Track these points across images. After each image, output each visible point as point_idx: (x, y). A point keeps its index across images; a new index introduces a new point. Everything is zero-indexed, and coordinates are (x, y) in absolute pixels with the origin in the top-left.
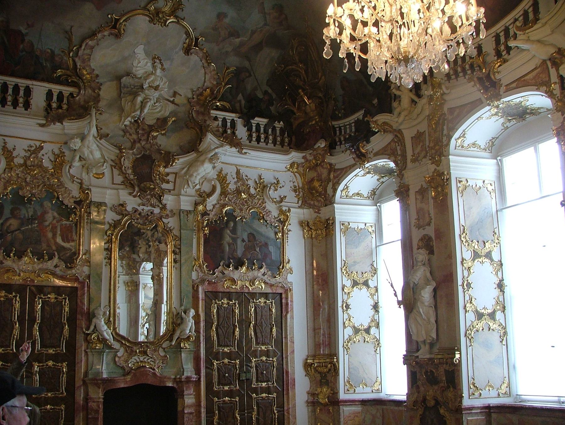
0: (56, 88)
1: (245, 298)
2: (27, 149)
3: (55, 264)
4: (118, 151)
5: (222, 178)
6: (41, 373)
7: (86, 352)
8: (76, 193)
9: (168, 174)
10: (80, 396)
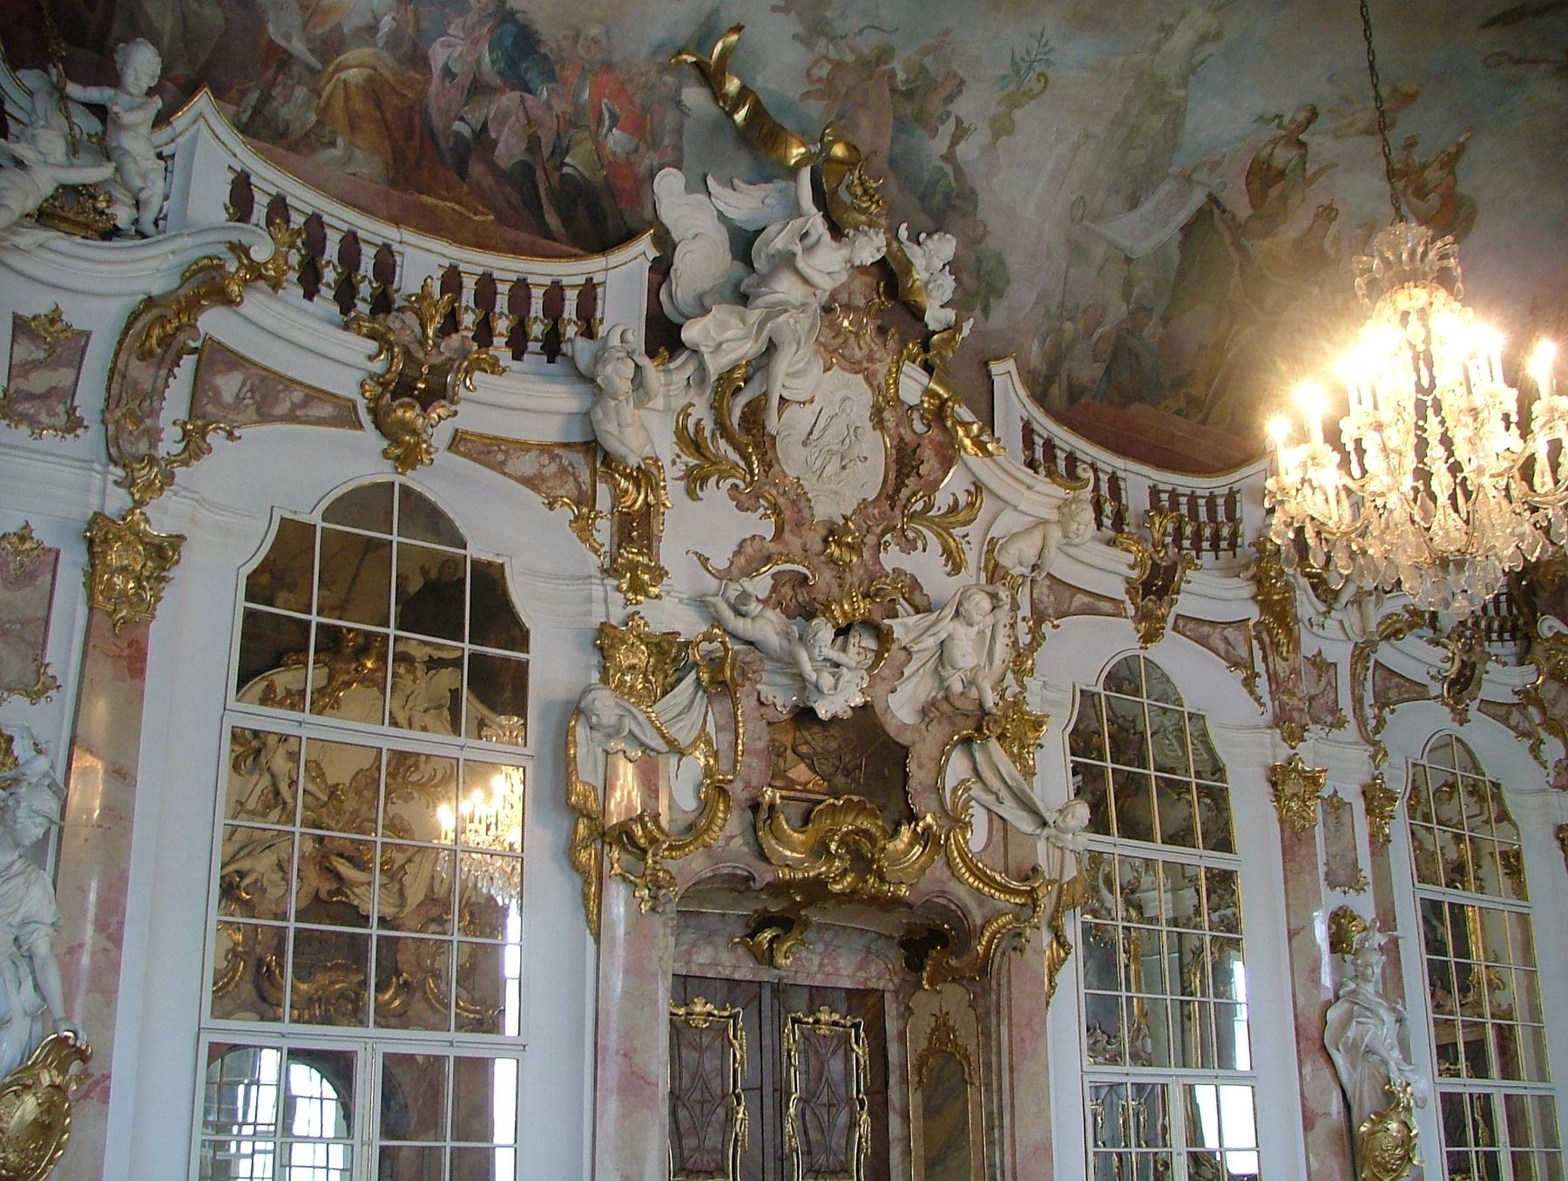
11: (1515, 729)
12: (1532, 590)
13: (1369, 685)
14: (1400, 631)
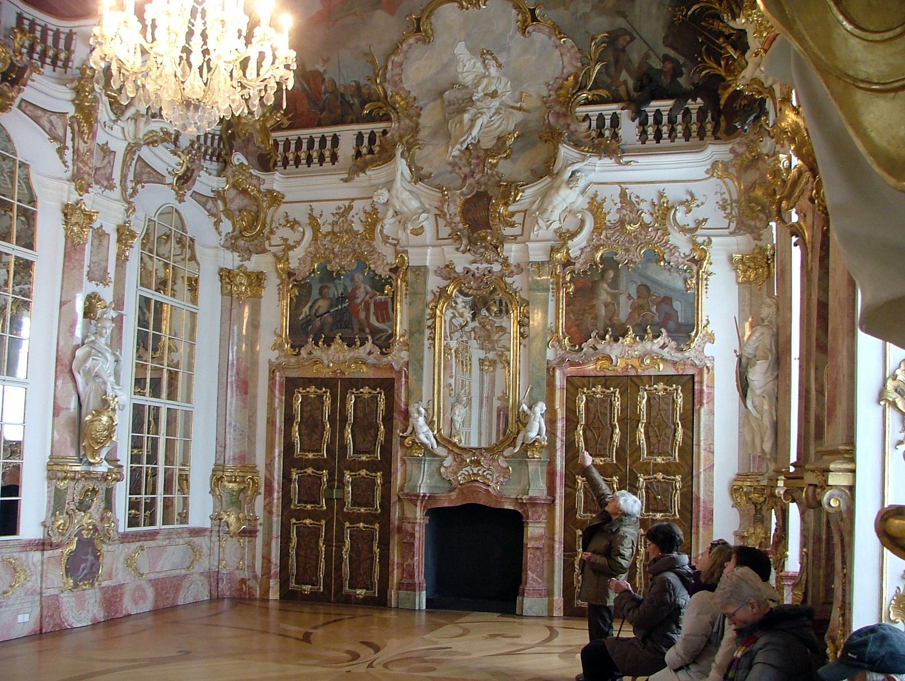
0: (366, 128)
1: (629, 383)
2: (335, 212)
4: (441, 195)
5: (596, 207)
6: (354, 484)
8: (391, 259)
9: (512, 214)
10: (396, 513)
11: (208, 211)
12: (232, 137)
13: (132, 169)
14: (156, 141)
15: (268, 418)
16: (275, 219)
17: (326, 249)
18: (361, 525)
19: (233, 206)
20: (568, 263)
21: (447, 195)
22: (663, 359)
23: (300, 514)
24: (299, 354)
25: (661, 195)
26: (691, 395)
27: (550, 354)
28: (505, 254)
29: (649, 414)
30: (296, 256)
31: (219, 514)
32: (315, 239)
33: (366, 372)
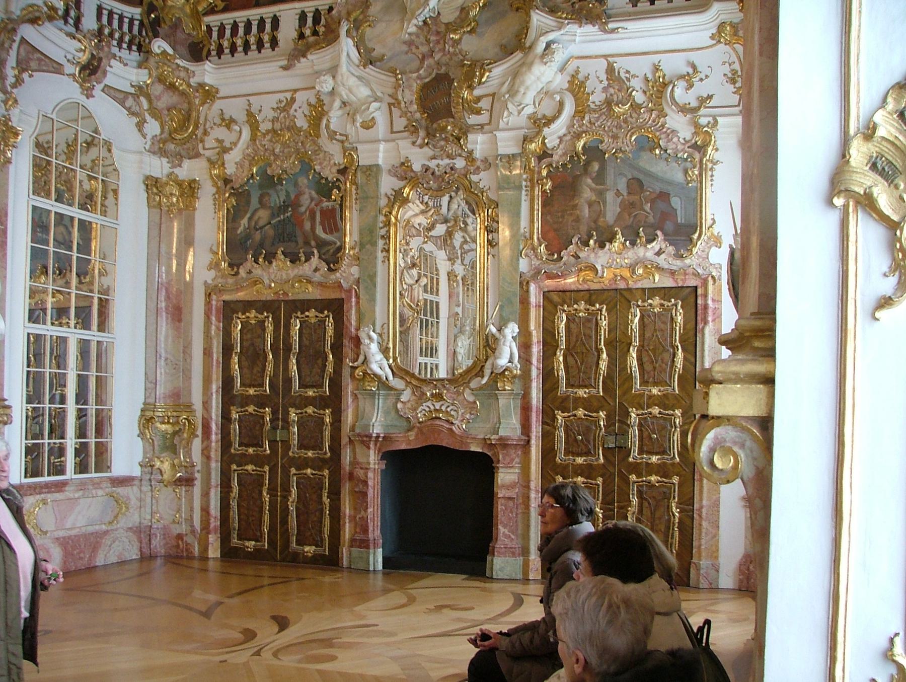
1: (619, 298)
2: (275, 106)
3: (314, 267)
4: (394, 80)
5: (577, 87)
7: (355, 397)
8: (339, 159)
9: (478, 99)
11: (128, 109)
15: (205, 349)
16: (210, 118)
17: (266, 150)
18: (309, 471)
19: (161, 104)
20: (544, 155)
21: (401, 79)
22: (659, 268)
23: (243, 459)
24: (237, 273)
25: (656, 68)
26: (694, 310)
27: (524, 265)
28: (470, 147)
29: (642, 335)
30: (232, 159)
31: (151, 460)
32: (253, 139)
33: (312, 293)
